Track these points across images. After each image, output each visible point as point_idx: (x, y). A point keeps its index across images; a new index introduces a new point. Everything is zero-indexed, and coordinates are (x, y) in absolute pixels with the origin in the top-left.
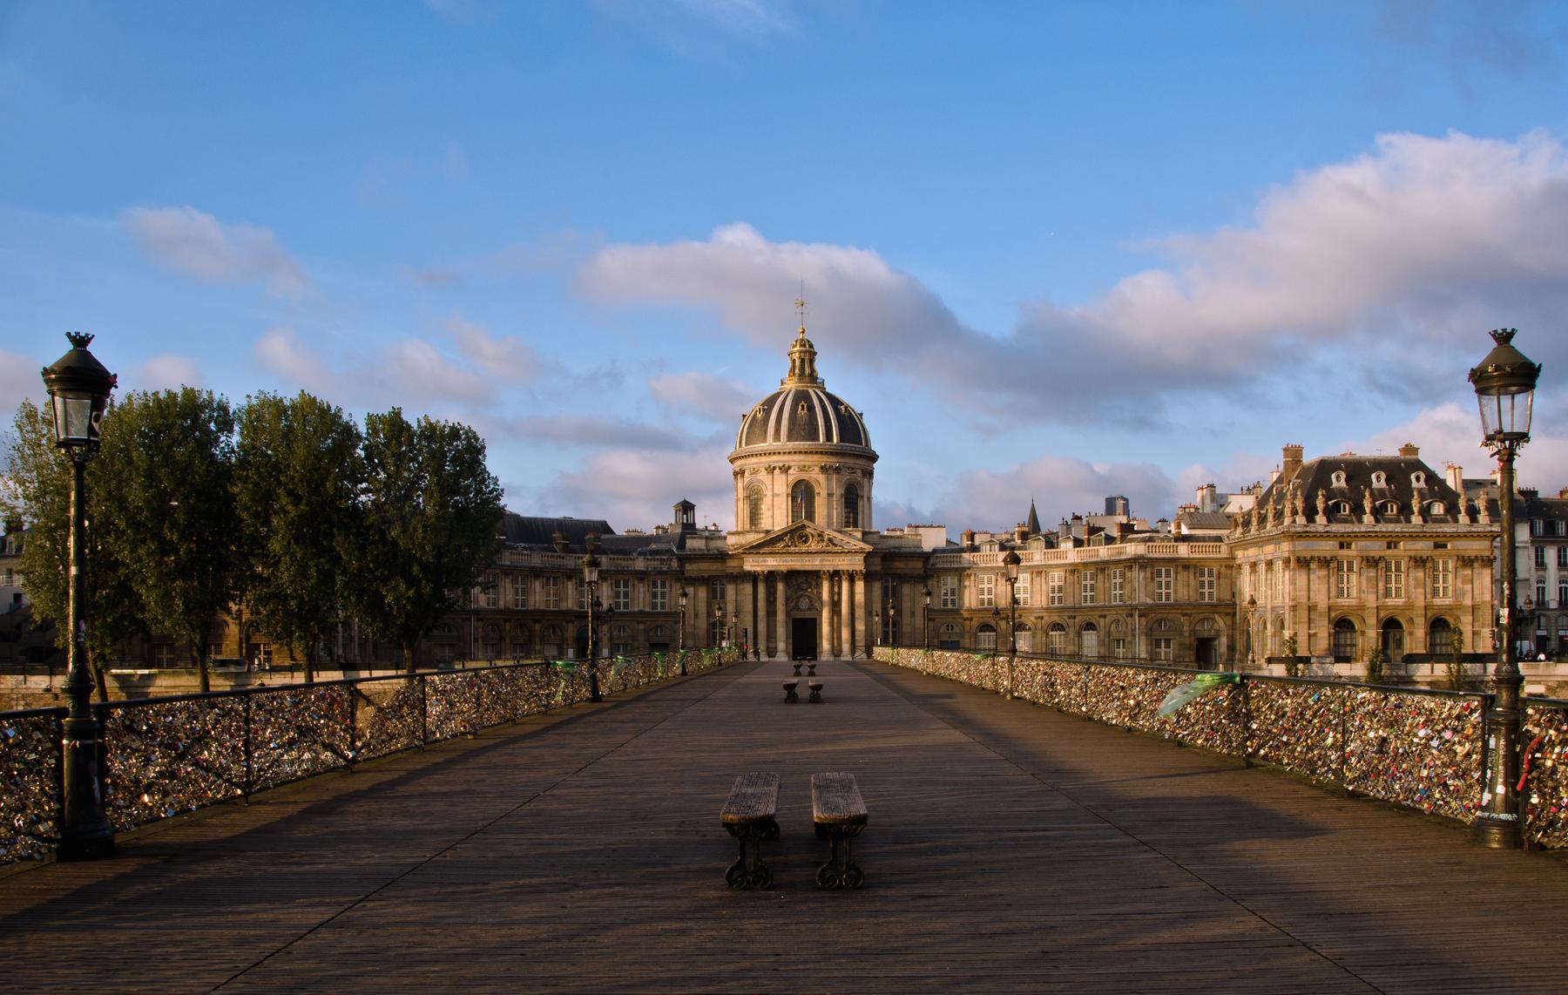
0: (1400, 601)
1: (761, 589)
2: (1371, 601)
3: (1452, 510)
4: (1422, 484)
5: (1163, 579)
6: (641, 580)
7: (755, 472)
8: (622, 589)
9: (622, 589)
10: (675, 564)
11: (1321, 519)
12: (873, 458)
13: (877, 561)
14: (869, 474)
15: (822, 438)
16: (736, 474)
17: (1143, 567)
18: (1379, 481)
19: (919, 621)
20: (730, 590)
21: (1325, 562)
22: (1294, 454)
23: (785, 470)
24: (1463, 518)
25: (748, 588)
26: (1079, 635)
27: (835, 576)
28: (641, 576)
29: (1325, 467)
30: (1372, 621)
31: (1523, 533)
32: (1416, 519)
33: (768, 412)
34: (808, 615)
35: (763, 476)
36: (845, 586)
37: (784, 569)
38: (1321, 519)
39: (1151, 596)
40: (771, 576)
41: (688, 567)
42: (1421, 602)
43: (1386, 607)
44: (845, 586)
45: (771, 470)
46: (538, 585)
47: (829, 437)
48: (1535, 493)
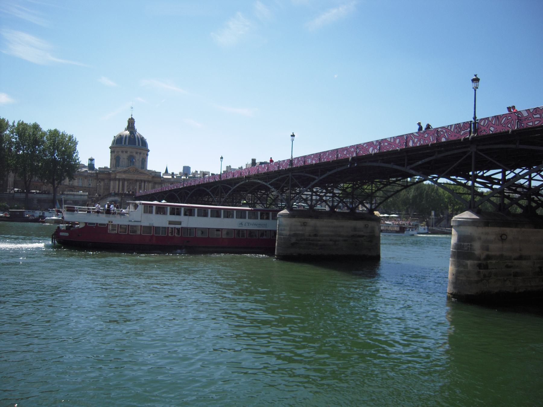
6: (86, 178)
7: (118, 152)
12: (149, 151)
13: (150, 178)
14: (147, 155)
15: (137, 144)
16: (111, 152)
20: (112, 182)
22: (254, 161)
23: (126, 152)
25: (117, 182)
27: (141, 181)
29: (261, 163)
35: (120, 153)
36: (143, 184)
40: (124, 180)
44: (143, 184)
45: (122, 152)
47: (139, 145)
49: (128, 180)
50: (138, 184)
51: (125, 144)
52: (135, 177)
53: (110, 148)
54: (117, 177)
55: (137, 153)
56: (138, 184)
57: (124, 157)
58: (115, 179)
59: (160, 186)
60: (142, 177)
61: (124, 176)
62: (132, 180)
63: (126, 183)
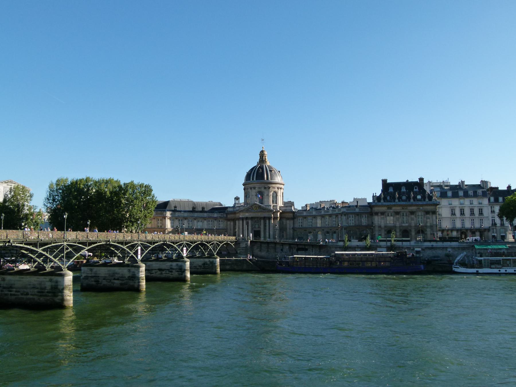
0: (407, 224)
1: (245, 222)
2: (398, 224)
3: (424, 198)
4: (417, 190)
5: (351, 219)
6: (216, 220)
7: (248, 189)
8: (210, 223)
9: (210, 223)
10: (225, 215)
11: (382, 201)
16: (244, 189)
17: (345, 215)
18: (403, 189)
19: (291, 231)
20: (237, 222)
21: (383, 213)
22: (384, 182)
23: (254, 188)
24: (427, 200)
25: (241, 222)
26: (332, 235)
27: (264, 218)
28: (216, 219)
30: (398, 230)
31: (485, 201)
32: (412, 200)
33: (251, 172)
34: (258, 229)
35: (249, 190)
36: (267, 221)
37: (250, 216)
38: (382, 201)
39: (348, 224)
40: (247, 218)
41: (228, 216)
42: (413, 225)
43: (402, 226)
44: (267, 221)
45: (251, 188)
46: (186, 222)
48: (498, 188)
49: (252, 218)
50: (262, 221)
51: (253, 179)
52: (259, 215)
53: (244, 185)
54: (241, 216)
55: (265, 188)
56: (262, 221)
57: (253, 192)
58: (239, 219)
59: (292, 221)
60: (266, 215)
61: (247, 215)
62: (257, 218)
63: (250, 222)
